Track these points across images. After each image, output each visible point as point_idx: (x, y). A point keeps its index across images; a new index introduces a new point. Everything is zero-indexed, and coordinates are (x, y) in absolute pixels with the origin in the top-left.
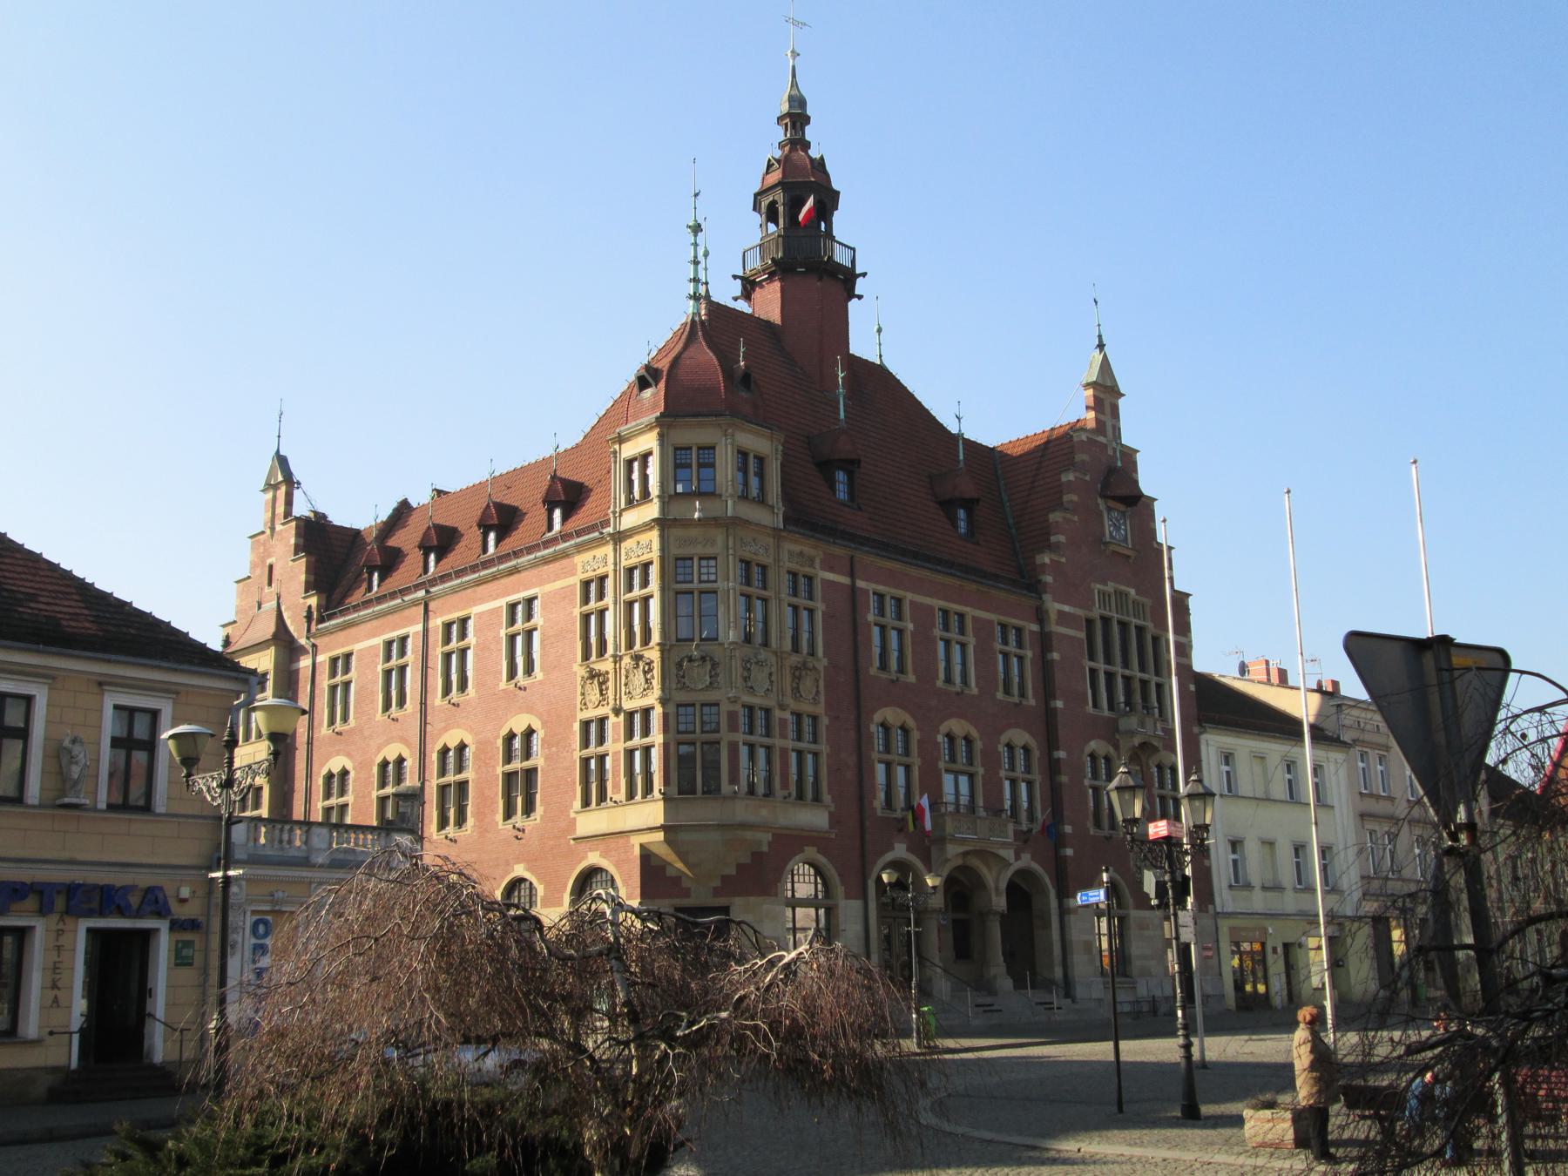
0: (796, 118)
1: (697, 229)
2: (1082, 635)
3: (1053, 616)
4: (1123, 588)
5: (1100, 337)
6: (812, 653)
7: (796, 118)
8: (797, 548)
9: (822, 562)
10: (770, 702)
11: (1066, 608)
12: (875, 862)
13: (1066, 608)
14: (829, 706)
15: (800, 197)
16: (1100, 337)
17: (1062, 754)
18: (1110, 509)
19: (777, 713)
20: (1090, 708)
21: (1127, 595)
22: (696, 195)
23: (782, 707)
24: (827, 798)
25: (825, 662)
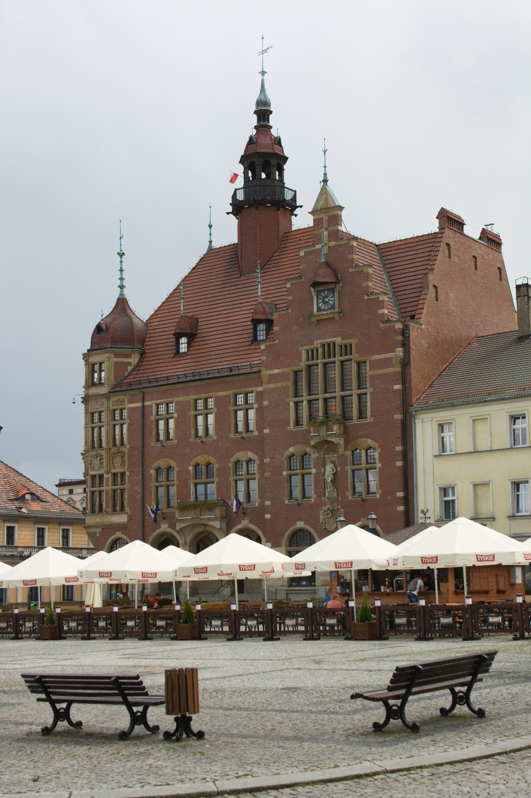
0: (263, 114)
1: (121, 255)
2: (290, 384)
3: (264, 380)
4: (328, 340)
5: (325, 174)
6: (122, 444)
7: (263, 114)
8: (116, 399)
9: (128, 400)
10: (101, 472)
11: (276, 371)
12: (151, 535)
13: (276, 371)
14: (130, 466)
15: (263, 159)
16: (325, 174)
17: (267, 460)
18: (318, 293)
19: (105, 476)
20: (291, 427)
21: (334, 344)
22: (121, 238)
23: (107, 473)
24: (127, 509)
25: (128, 446)
